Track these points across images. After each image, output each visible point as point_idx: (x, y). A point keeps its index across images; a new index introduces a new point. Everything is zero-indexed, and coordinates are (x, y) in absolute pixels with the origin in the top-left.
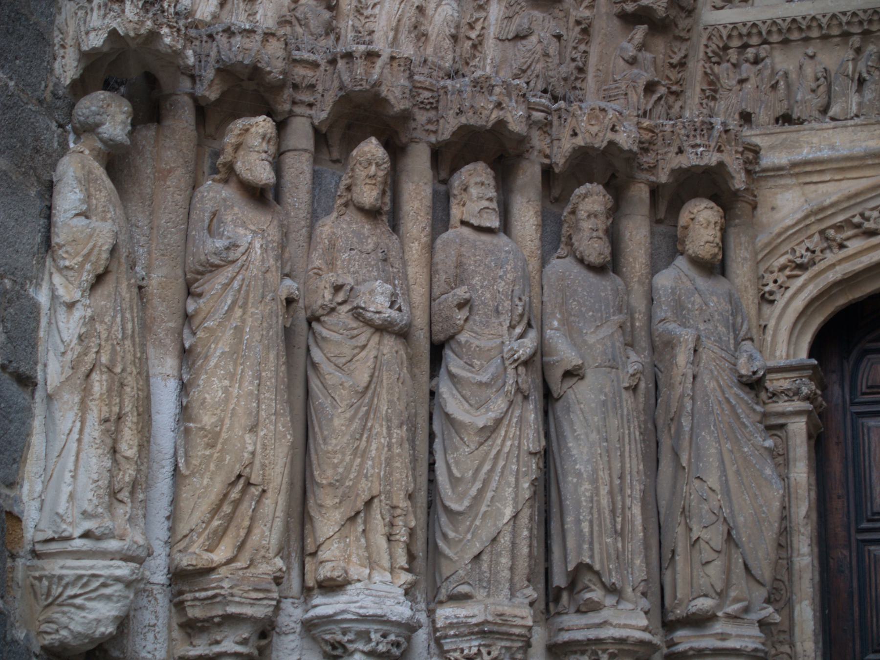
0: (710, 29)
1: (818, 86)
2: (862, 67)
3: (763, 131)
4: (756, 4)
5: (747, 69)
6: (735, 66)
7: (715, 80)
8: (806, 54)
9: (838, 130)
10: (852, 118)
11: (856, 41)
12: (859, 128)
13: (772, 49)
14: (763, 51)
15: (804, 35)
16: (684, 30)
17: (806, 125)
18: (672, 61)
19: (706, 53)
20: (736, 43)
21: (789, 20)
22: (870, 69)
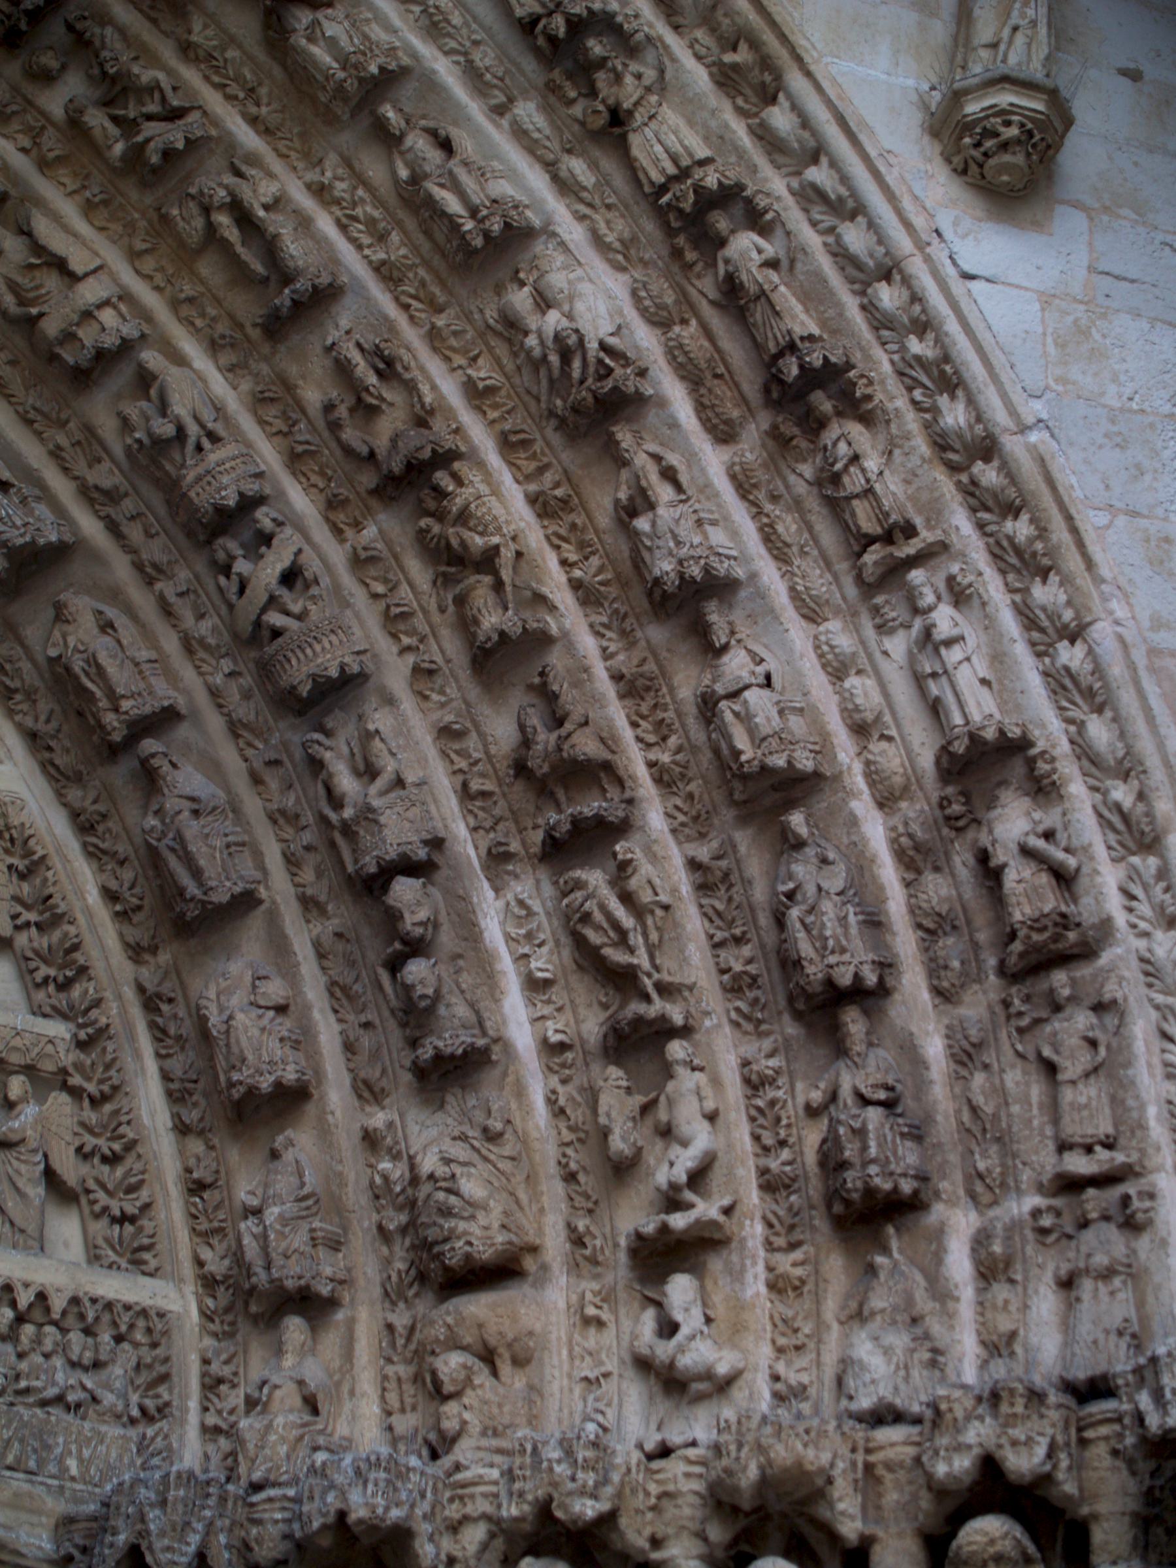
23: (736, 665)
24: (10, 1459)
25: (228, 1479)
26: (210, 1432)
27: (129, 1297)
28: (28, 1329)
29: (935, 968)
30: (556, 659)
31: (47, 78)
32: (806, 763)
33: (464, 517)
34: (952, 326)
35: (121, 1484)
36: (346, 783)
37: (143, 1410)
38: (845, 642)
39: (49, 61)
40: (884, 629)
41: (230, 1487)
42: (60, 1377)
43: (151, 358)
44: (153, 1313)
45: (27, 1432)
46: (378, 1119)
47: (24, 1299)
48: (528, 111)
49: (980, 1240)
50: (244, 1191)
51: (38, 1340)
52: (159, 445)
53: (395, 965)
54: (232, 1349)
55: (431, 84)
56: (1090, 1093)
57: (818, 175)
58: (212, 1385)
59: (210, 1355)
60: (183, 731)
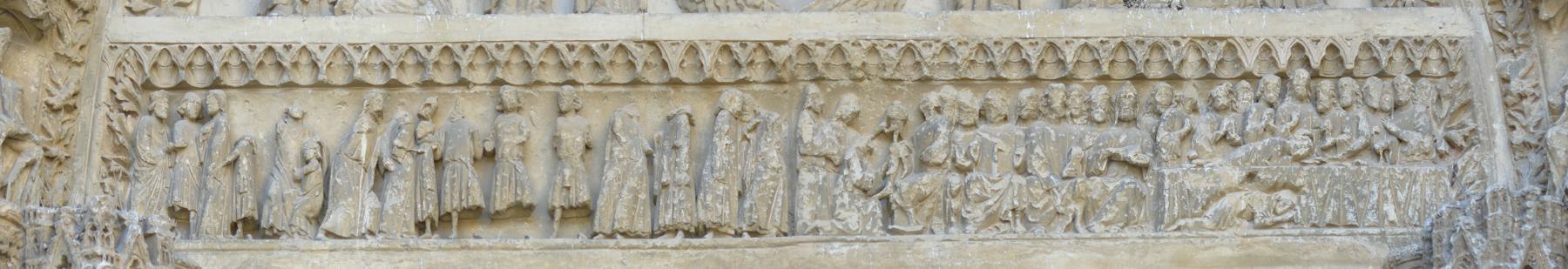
0: (121, 49)
1: (307, 174)
2: (382, 146)
3: (209, 245)
4: (202, 14)
5: (185, 131)
6: (160, 119)
7: (127, 144)
8: (287, 114)
9: (337, 254)
10: (363, 236)
11: (376, 97)
12: (374, 255)
13: (228, 98)
14: (214, 100)
15: (286, 79)
16: (74, 45)
17: (284, 241)
18: (52, 101)
19: (113, 92)
20: (164, 79)
21: (261, 48)
22: (397, 152)
24: (1329, 217)
25: (1544, 192)
26: (1518, 150)
27: (1419, 32)
28: (1326, 86)
35: (1439, 216)
37: (1451, 143)
41: (1547, 198)
42: (1363, 125)
44: (1444, 43)
45: (1338, 187)
47: (1316, 55)
51: (1337, 94)
54: (1529, 63)
58: (1513, 104)
59: (1507, 73)
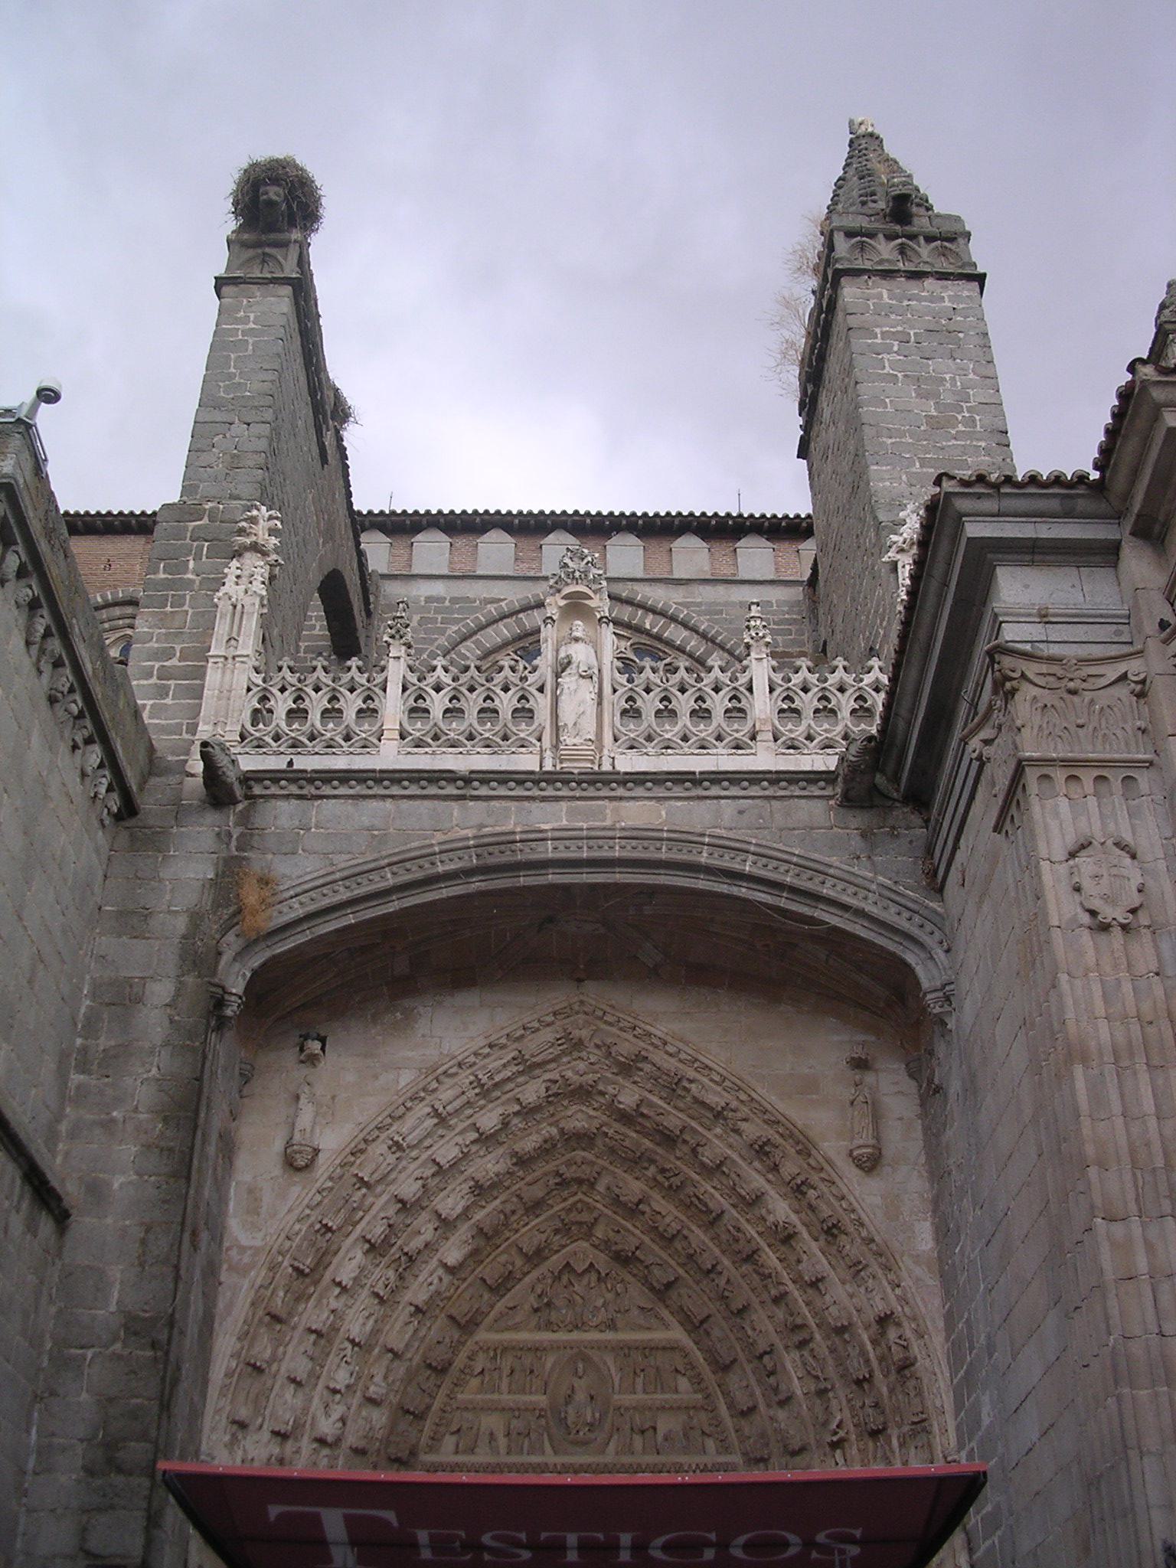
23: (827, 1297)
29: (882, 1371)
30: (789, 1297)
31: (646, 1169)
32: (846, 1323)
33: (762, 1266)
34: (860, 1211)
36: (750, 1332)
38: (850, 1290)
39: (646, 1164)
40: (859, 1286)
43: (685, 1232)
46: (772, 1413)
48: (757, 1164)
49: (899, 1438)
50: (746, 1431)
52: (692, 1255)
53: (768, 1376)
55: (734, 1161)
56: (917, 1400)
57: (822, 1175)
60: (712, 1319)
